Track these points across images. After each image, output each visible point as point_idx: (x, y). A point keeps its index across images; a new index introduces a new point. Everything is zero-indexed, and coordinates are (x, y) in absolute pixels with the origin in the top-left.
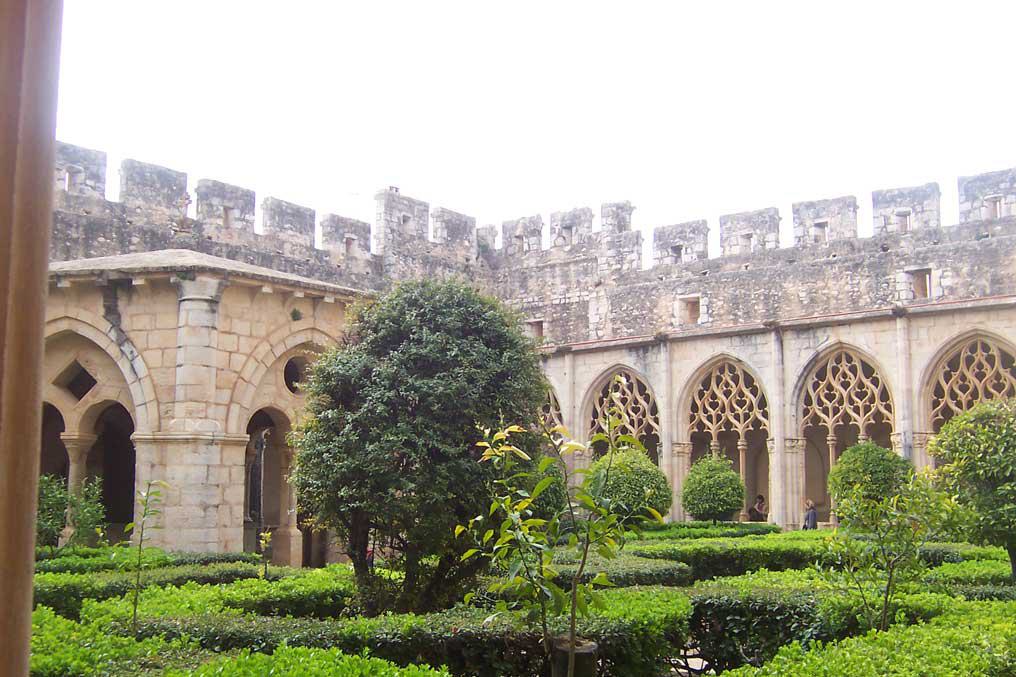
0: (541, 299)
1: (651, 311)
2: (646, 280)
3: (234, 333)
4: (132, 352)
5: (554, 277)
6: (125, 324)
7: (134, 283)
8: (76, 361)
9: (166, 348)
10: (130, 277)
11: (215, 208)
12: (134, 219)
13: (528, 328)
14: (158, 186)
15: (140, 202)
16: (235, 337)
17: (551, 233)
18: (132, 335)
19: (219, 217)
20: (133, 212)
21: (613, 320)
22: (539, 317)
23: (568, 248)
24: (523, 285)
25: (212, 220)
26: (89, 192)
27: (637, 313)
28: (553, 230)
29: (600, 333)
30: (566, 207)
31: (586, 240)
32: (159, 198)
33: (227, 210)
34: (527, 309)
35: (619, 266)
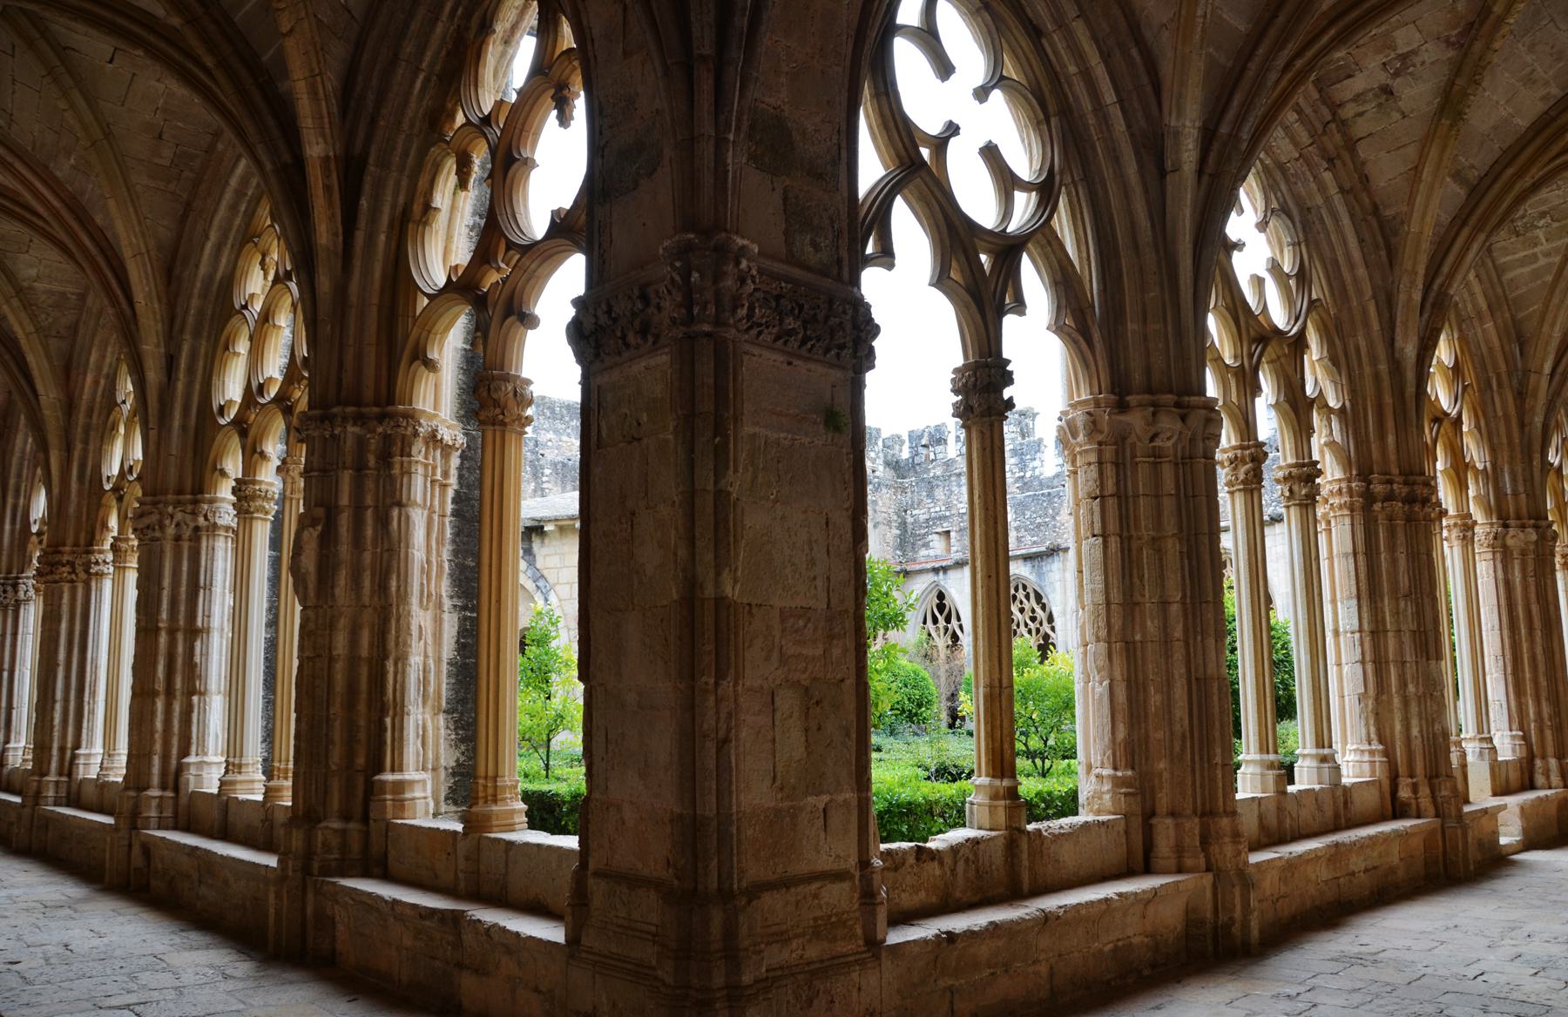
0: (948, 509)
1: (1053, 518)
2: (1048, 487)
5: (959, 486)
6: (539, 564)
7: (546, 529)
10: (542, 524)
13: (936, 537)
14: (567, 419)
15: (551, 435)
18: (545, 573)
20: (545, 445)
22: (946, 526)
24: (930, 495)
32: (569, 431)
34: (933, 519)
35: (1022, 474)
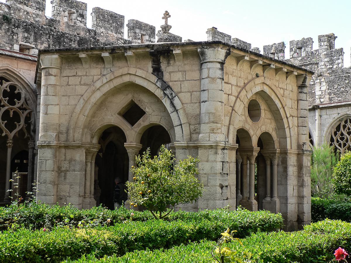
3: (230, 84)
4: (172, 94)
6: (166, 77)
7: (174, 52)
8: (132, 100)
9: (193, 92)
11: (137, 35)
12: (100, 38)
14: (111, 22)
15: (102, 30)
16: (230, 86)
17: (290, 51)
18: (171, 84)
19: (139, 39)
20: (99, 35)
21: (330, 94)
23: (300, 58)
25: (136, 40)
26: (79, 24)
27: (343, 90)
28: (291, 50)
29: (322, 100)
30: (298, 38)
31: (310, 54)
32: (112, 28)
33: (142, 35)
35: (331, 66)
